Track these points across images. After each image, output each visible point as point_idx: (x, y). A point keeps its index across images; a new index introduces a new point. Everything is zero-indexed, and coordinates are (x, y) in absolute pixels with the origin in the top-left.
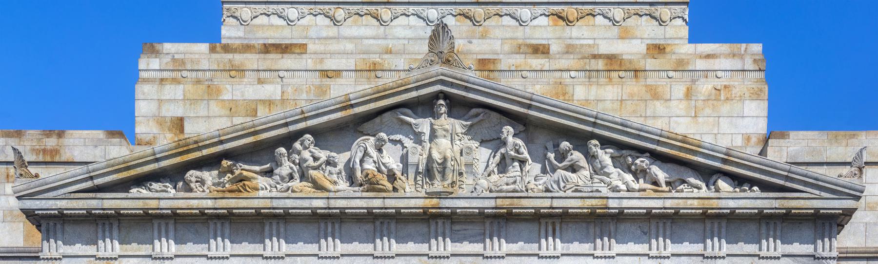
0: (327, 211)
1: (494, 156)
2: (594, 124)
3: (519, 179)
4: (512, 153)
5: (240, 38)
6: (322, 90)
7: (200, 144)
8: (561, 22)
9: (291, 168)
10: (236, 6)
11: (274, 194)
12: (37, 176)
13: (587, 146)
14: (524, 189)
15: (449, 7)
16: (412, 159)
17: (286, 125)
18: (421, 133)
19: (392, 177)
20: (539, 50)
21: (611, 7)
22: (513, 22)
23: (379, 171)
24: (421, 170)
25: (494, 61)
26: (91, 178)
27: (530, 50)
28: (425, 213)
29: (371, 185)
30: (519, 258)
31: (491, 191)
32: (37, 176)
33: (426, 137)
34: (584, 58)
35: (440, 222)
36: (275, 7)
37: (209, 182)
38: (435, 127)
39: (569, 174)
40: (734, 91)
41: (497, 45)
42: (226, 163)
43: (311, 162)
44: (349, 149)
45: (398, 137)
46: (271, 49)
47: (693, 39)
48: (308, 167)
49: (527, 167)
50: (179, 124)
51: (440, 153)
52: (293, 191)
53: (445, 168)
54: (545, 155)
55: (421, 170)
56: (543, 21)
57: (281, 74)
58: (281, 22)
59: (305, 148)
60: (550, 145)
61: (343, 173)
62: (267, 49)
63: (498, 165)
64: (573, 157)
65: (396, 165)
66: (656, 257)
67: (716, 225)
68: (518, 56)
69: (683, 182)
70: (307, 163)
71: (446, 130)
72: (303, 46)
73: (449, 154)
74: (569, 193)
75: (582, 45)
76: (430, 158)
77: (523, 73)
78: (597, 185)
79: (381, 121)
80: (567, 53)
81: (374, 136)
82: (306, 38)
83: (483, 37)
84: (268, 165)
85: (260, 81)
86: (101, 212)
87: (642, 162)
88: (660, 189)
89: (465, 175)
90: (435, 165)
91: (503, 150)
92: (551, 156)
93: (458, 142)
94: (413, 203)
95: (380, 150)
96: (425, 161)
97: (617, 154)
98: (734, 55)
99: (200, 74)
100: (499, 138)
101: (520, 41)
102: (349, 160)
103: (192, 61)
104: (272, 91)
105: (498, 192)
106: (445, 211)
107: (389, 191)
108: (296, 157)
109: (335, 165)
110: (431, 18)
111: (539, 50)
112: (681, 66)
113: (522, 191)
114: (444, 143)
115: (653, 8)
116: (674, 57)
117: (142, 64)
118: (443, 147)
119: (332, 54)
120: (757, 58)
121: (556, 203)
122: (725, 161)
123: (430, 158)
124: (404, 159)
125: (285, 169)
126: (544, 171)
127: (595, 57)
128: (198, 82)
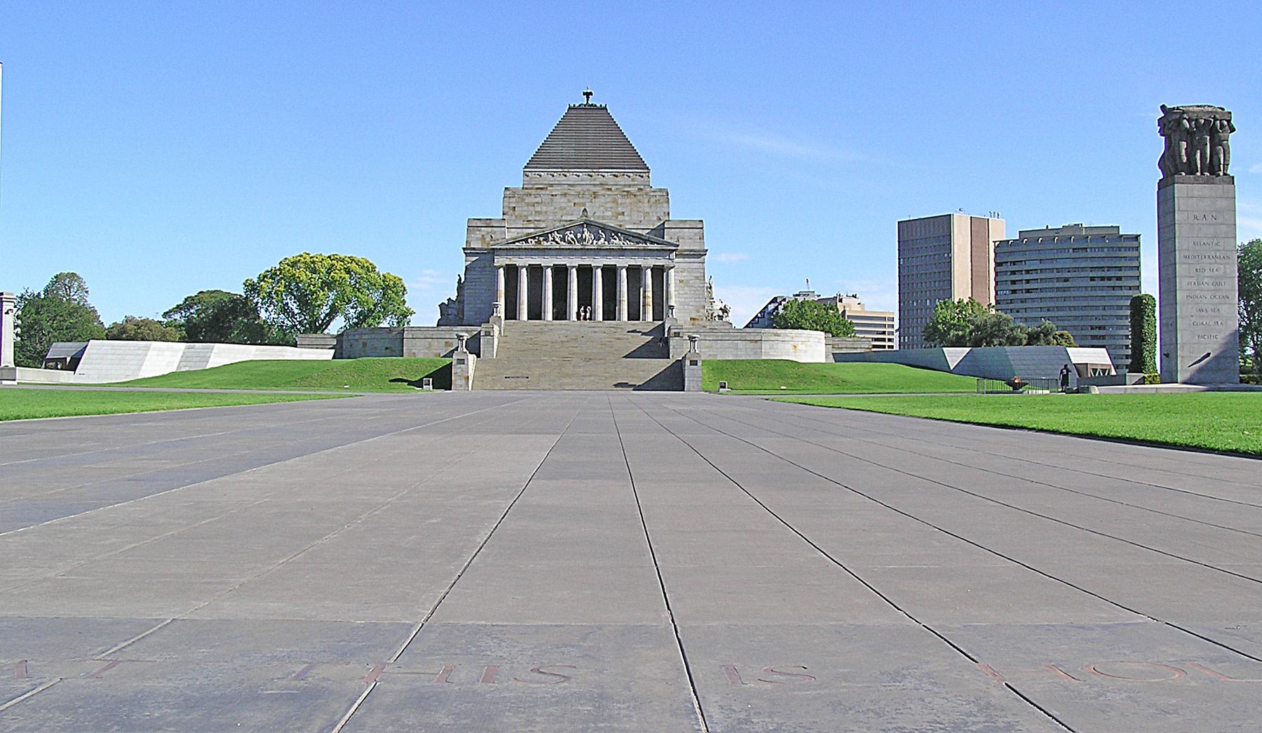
29: (570, 243)
62: (537, 189)
85: (536, 197)
112: (647, 194)
127: (624, 191)
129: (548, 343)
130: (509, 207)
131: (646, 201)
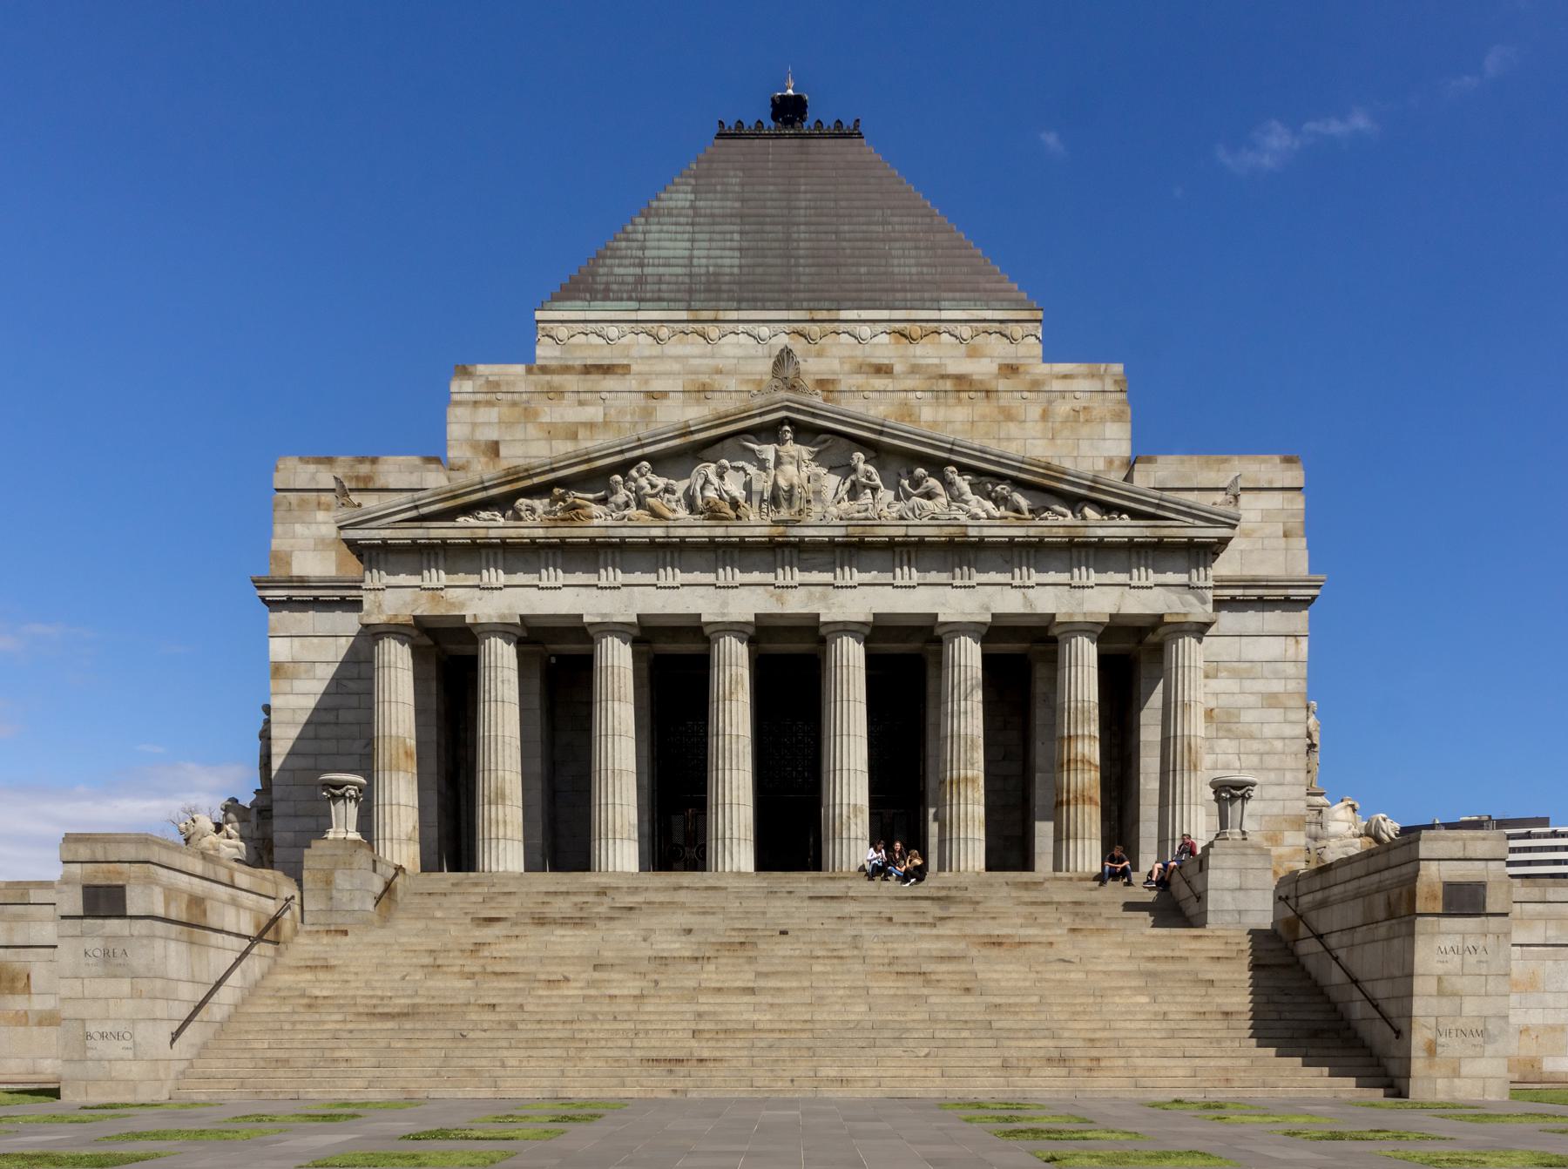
0: (666, 540)
1: (844, 484)
2: (951, 451)
3: (871, 506)
4: (864, 480)
5: (556, 358)
6: (647, 414)
7: (531, 472)
8: (904, 340)
9: (627, 496)
10: (551, 325)
11: (610, 522)
12: (360, 505)
13: (943, 472)
14: (876, 517)
15: (782, 325)
16: (756, 487)
17: (622, 452)
18: (765, 460)
19: (735, 504)
20: (882, 370)
21: (958, 325)
22: (852, 340)
23: (721, 498)
24: (765, 498)
25: (833, 382)
26: (416, 507)
27: (872, 370)
28: (770, 542)
29: (713, 513)
30: (872, 588)
31: (841, 519)
32: (360, 505)
33: (771, 464)
34: (930, 378)
35: (787, 552)
36: (594, 325)
37: (540, 510)
38: (781, 453)
39: (924, 502)
40: (1094, 413)
41: (836, 365)
42: (557, 491)
43: (648, 490)
44: (689, 477)
45: (740, 464)
46: (592, 370)
47: (1048, 358)
48: (645, 495)
49: (880, 495)
50: (494, 449)
51: (786, 480)
52: (629, 520)
53: (791, 496)
54: (899, 482)
55: (765, 498)
56: (884, 338)
57: (603, 395)
58: (601, 341)
59: (642, 475)
60: (903, 471)
61: (682, 501)
62: (588, 370)
63: (848, 492)
64: (929, 483)
65: (739, 493)
66: (1020, 587)
67: (1083, 554)
68: (859, 376)
69: (1048, 509)
70: (644, 491)
71: (792, 457)
72: (627, 367)
73: (796, 481)
74: (925, 521)
75: (928, 365)
76: (775, 485)
77: (866, 394)
78: (955, 513)
79: (722, 448)
80: (912, 372)
81: (715, 462)
82: (628, 356)
83: (819, 355)
84: (603, 493)
85: (581, 403)
86: (427, 541)
87: (1003, 489)
88: (1022, 516)
89: (813, 503)
90: (782, 493)
91: (853, 477)
92: (906, 483)
93: (805, 469)
94: (758, 531)
95: (721, 477)
96: (770, 489)
97: (975, 481)
98: (1093, 376)
99: (516, 396)
100: (849, 465)
101: (860, 360)
102: (689, 488)
103: (508, 383)
104: (594, 413)
105: (849, 519)
106: (792, 539)
107: (732, 519)
108: (632, 485)
109: (673, 492)
110: (762, 335)
111: (882, 370)
112: (1036, 386)
113: (874, 519)
114: (790, 469)
115: (1003, 326)
116: (1028, 377)
117: (454, 387)
118: (789, 475)
119: (659, 374)
120: (1118, 378)
121: (912, 531)
122: (1091, 488)
123: (775, 485)
124: (748, 486)
125: (622, 495)
126: (897, 498)
127: (943, 377)
128: (514, 404)
129: (568, 970)
130: (475, 445)
131: (1035, 412)
